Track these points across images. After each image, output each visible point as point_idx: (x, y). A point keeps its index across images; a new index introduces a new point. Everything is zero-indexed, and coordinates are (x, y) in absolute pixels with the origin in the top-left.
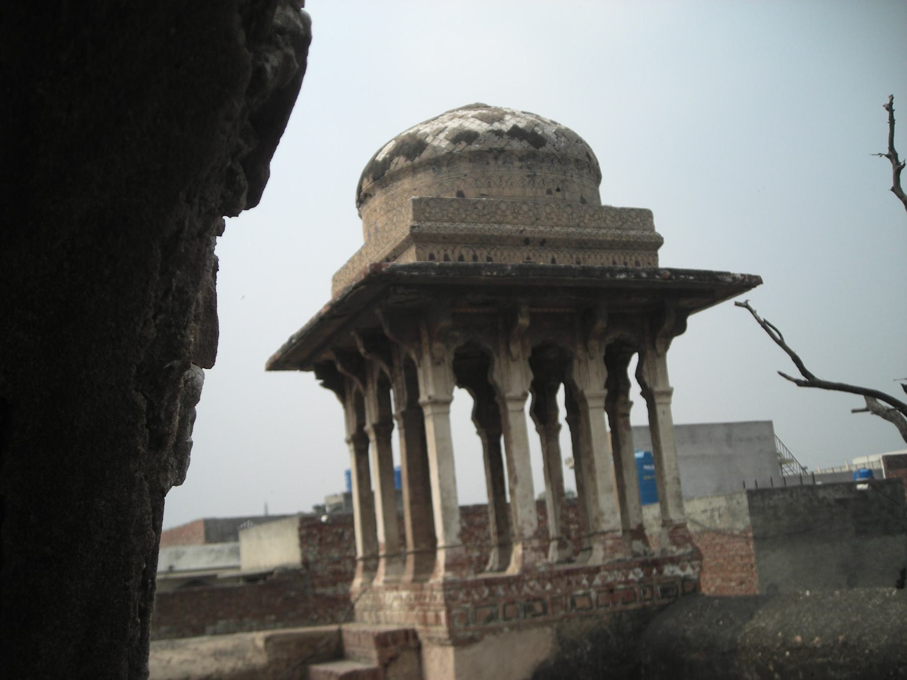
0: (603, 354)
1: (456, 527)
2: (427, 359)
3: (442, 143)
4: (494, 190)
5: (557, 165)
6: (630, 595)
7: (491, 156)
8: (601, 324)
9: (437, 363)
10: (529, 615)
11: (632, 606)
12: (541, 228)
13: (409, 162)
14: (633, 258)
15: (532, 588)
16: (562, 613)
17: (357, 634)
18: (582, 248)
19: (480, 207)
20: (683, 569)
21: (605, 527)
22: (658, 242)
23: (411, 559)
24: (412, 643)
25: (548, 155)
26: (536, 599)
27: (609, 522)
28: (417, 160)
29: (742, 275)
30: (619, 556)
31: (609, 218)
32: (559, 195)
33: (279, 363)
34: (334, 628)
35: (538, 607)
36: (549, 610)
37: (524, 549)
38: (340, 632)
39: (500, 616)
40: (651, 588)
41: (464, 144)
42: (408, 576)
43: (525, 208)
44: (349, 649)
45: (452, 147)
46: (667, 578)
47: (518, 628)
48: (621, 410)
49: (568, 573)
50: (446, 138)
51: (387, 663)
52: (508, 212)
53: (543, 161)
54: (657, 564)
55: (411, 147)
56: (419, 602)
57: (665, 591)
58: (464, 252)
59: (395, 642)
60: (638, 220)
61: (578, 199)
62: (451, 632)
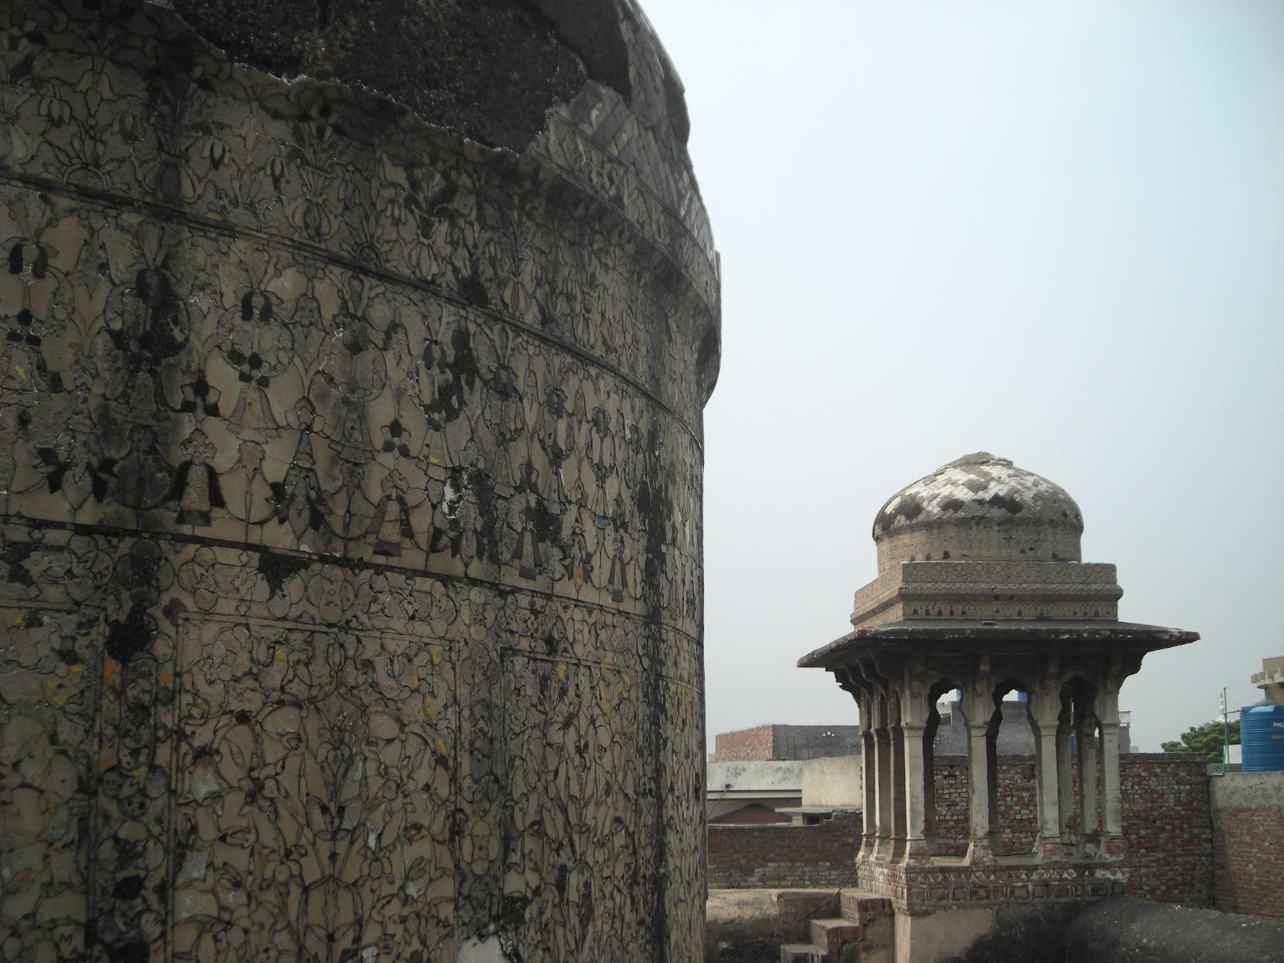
1: (921, 825)
2: (907, 692)
4: (974, 552)
6: (1062, 891)
8: (1053, 670)
9: (914, 697)
11: (1064, 900)
12: (1011, 585)
16: (1002, 899)
17: (850, 899)
19: (959, 568)
20: (1114, 873)
22: (1118, 594)
23: (892, 842)
24: (887, 910)
25: (1023, 519)
26: (981, 887)
28: (914, 521)
30: (1056, 858)
32: (1031, 554)
33: (811, 662)
34: (835, 890)
35: (982, 893)
38: (839, 894)
40: (1083, 887)
41: (951, 511)
42: (889, 858)
44: (844, 910)
47: (965, 907)
49: (1010, 868)
51: (865, 925)
53: (1018, 525)
55: (911, 508)
56: (893, 877)
57: (1095, 890)
59: (874, 908)
61: (1050, 554)
62: (909, 904)
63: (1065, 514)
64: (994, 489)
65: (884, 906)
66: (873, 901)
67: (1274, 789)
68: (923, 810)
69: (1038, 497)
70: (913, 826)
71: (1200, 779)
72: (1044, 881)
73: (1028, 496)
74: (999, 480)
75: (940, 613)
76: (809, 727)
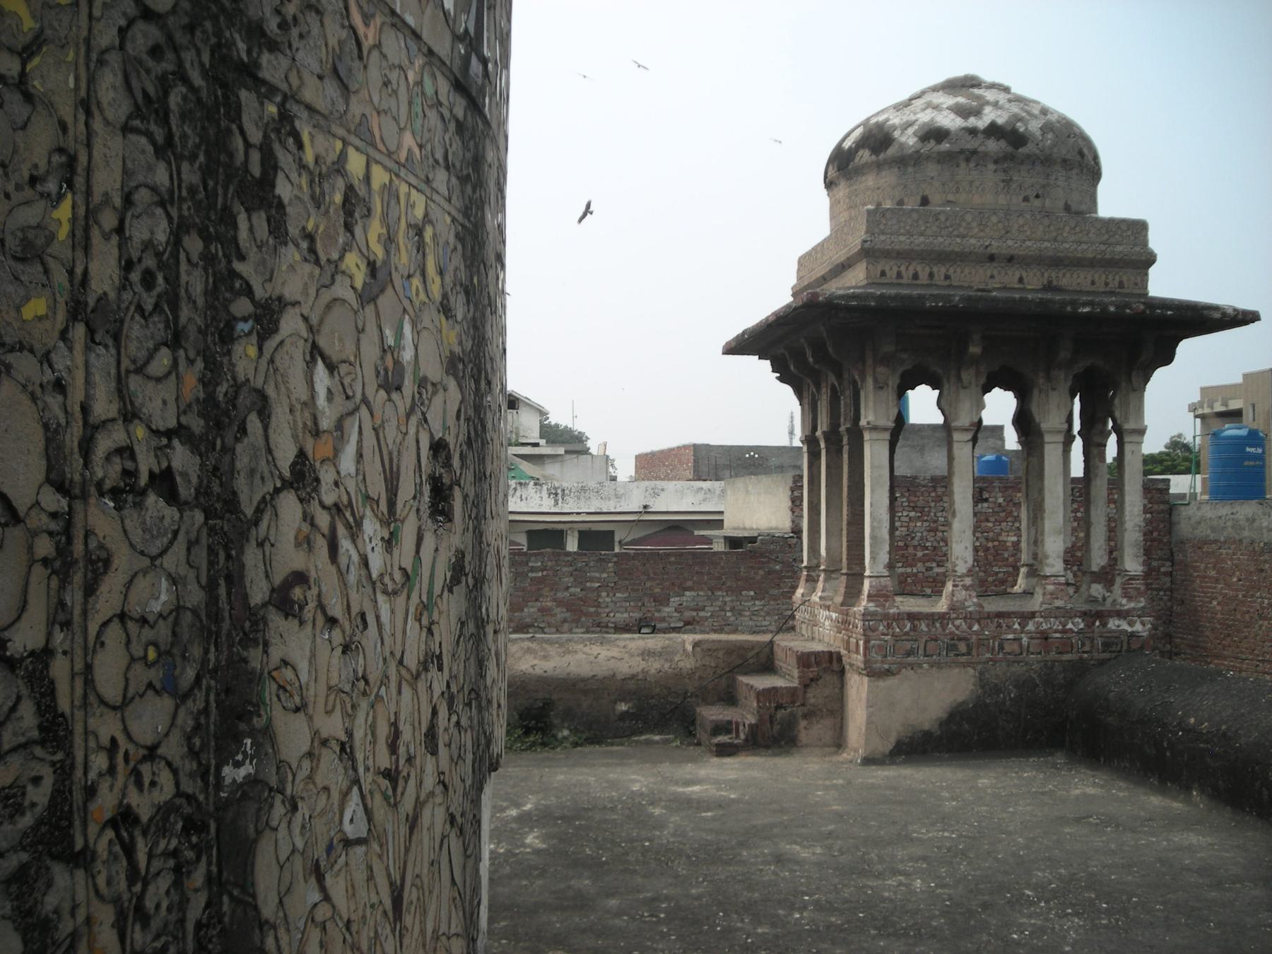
0: (1069, 383)
1: (884, 557)
2: (870, 382)
3: (909, 139)
4: (962, 197)
5: (1038, 168)
6: (1066, 646)
7: (962, 157)
8: (1064, 355)
9: (879, 387)
10: (952, 654)
12: (1010, 243)
13: (874, 157)
14: (1117, 278)
15: (957, 628)
16: (988, 655)
18: (1057, 266)
19: (942, 218)
20: (1131, 624)
21: (1048, 571)
22: (1150, 260)
23: (844, 578)
24: (835, 666)
25: (1028, 156)
26: (960, 639)
27: (1053, 566)
28: (882, 156)
29: (1235, 310)
30: (1059, 603)
31: (1093, 230)
32: (1037, 203)
34: (766, 638)
35: (962, 647)
36: (974, 652)
37: (954, 586)
38: (771, 642)
39: (921, 651)
40: (1092, 640)
41: (932, 142)
42: (839, 599)
43: (994, 219)
45: (920, 145)
46: (1111, 631)
47: (938, 665)
48: (1097, 439)
49: (1000, 615)
50: (915, 134)
52: (974, 224)
53: (1022, 163)
54: (1102, 616)
55: (876, 139)
56: (844, 624)
57: (1106, 645)
58: (919, 268)
59: (818, 664)
60: (1129, 233)
61: (1061, 204)
62: (866, 662)
63: (1081, 154)
64: (989, 116)
65: (831, 661)
66: (817, 655)
67: (1248, 520)
68: (887, 537)
69: (1047, 128)
70: (873, 558)
71: (1162, 507)
72: (1042, 632)
73: (1034, 126)
74: (996, 105)
75: (916, 276)
76: (732, 447)
